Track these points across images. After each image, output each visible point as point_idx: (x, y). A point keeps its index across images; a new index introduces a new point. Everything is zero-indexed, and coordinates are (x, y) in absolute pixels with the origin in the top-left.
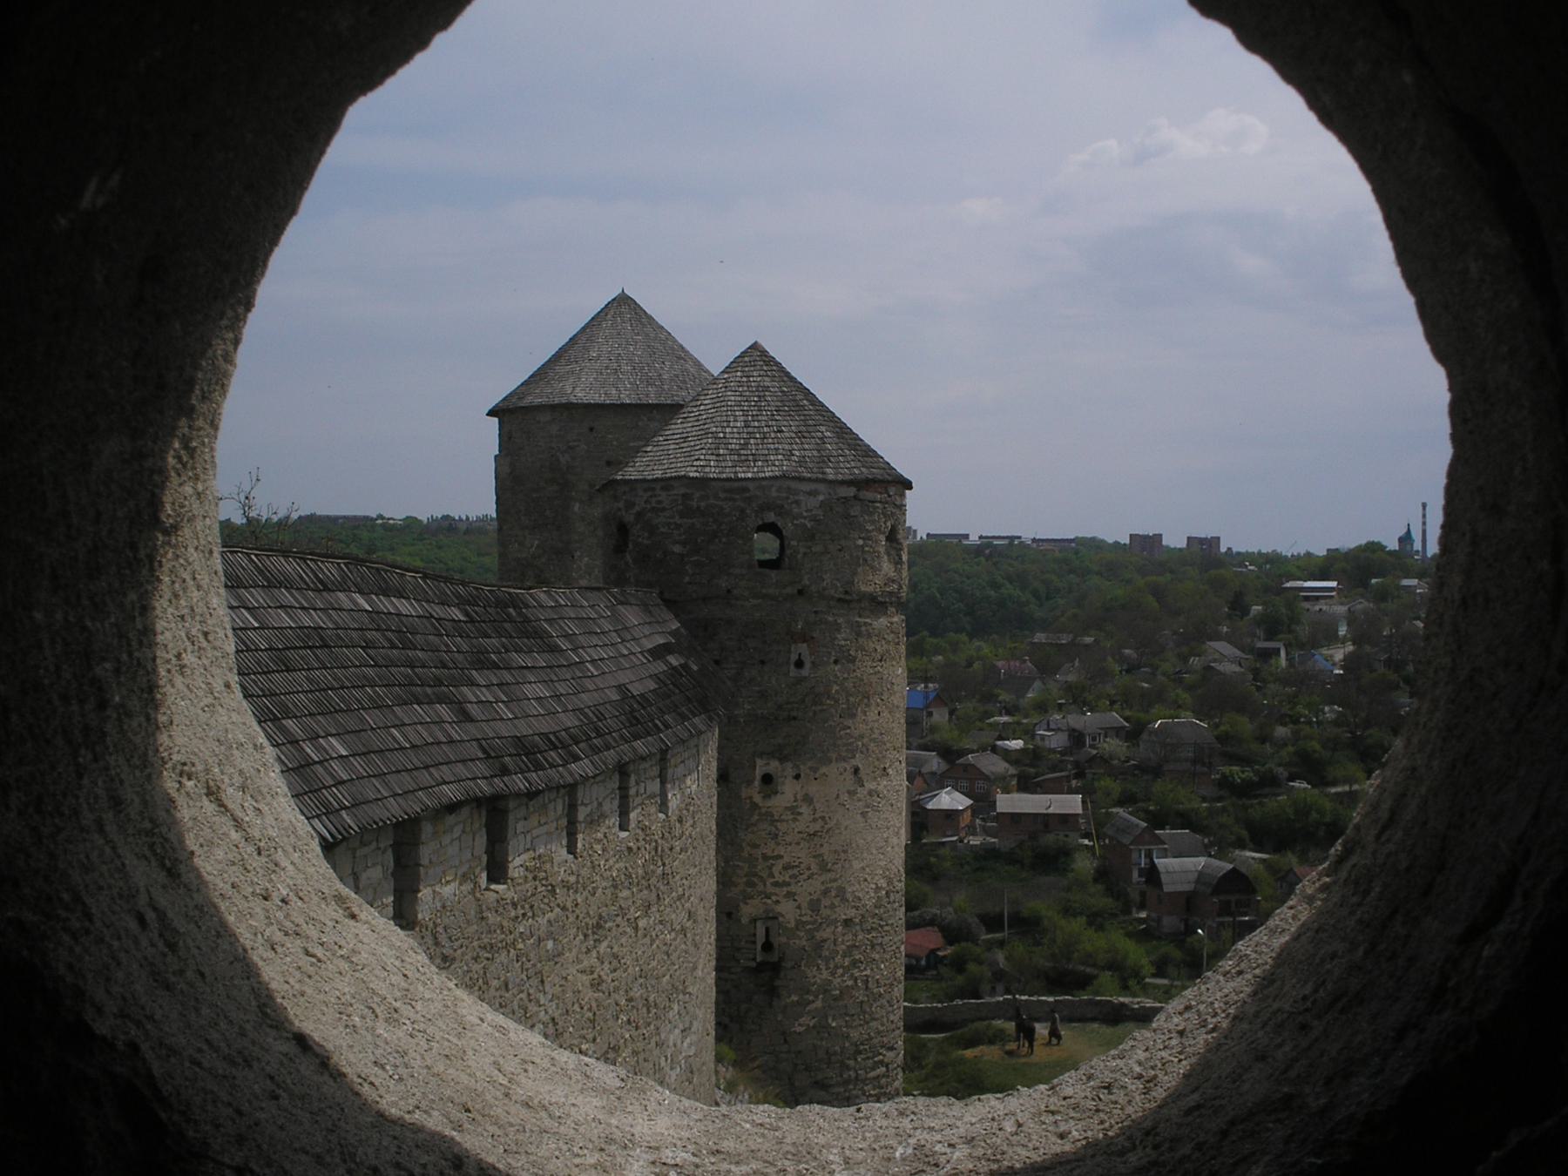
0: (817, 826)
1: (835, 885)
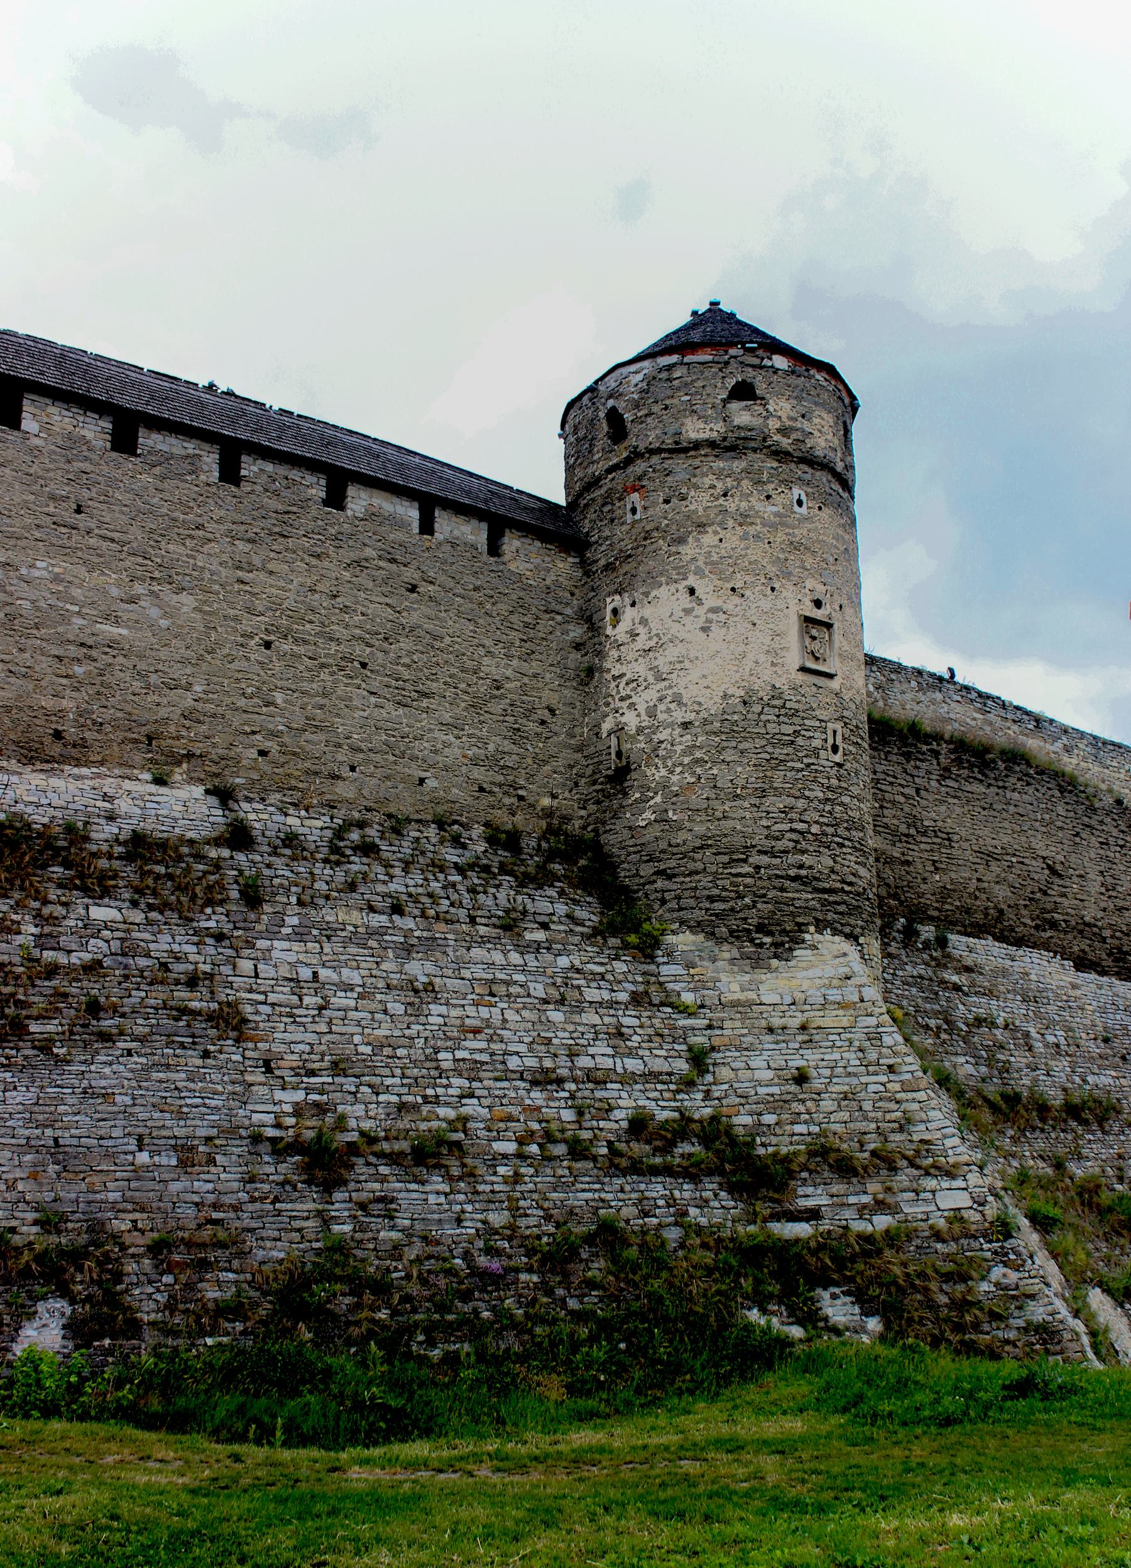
0: (652, 643)
1: (670, 692)
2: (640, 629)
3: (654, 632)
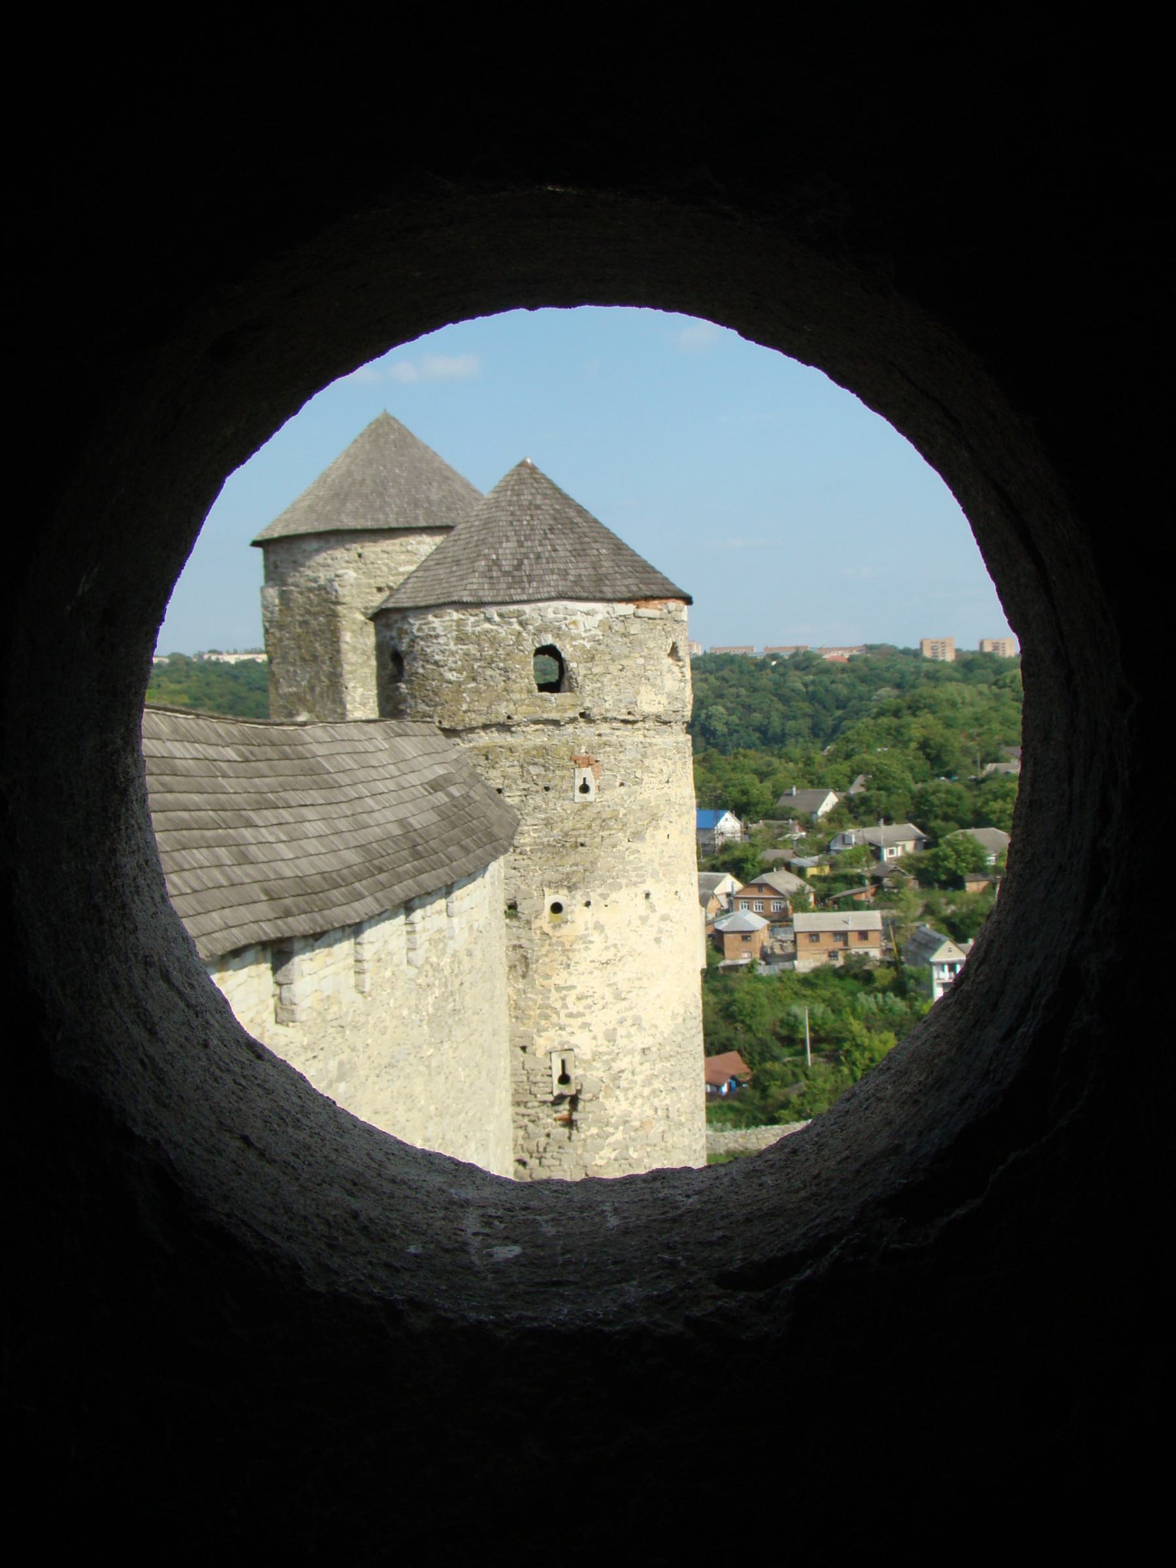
0: (609, 955)
1: (630, 1014)
2: (596, 937)
3: (610, 942)
